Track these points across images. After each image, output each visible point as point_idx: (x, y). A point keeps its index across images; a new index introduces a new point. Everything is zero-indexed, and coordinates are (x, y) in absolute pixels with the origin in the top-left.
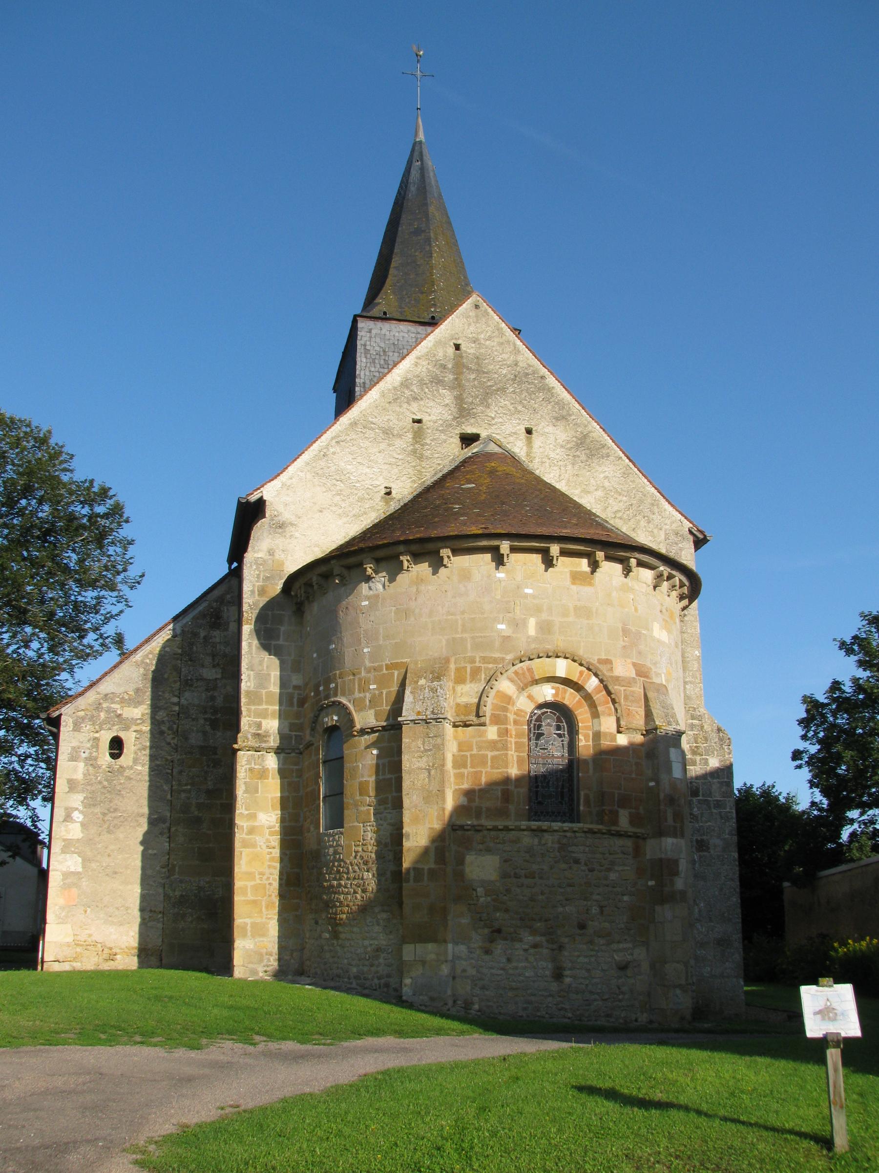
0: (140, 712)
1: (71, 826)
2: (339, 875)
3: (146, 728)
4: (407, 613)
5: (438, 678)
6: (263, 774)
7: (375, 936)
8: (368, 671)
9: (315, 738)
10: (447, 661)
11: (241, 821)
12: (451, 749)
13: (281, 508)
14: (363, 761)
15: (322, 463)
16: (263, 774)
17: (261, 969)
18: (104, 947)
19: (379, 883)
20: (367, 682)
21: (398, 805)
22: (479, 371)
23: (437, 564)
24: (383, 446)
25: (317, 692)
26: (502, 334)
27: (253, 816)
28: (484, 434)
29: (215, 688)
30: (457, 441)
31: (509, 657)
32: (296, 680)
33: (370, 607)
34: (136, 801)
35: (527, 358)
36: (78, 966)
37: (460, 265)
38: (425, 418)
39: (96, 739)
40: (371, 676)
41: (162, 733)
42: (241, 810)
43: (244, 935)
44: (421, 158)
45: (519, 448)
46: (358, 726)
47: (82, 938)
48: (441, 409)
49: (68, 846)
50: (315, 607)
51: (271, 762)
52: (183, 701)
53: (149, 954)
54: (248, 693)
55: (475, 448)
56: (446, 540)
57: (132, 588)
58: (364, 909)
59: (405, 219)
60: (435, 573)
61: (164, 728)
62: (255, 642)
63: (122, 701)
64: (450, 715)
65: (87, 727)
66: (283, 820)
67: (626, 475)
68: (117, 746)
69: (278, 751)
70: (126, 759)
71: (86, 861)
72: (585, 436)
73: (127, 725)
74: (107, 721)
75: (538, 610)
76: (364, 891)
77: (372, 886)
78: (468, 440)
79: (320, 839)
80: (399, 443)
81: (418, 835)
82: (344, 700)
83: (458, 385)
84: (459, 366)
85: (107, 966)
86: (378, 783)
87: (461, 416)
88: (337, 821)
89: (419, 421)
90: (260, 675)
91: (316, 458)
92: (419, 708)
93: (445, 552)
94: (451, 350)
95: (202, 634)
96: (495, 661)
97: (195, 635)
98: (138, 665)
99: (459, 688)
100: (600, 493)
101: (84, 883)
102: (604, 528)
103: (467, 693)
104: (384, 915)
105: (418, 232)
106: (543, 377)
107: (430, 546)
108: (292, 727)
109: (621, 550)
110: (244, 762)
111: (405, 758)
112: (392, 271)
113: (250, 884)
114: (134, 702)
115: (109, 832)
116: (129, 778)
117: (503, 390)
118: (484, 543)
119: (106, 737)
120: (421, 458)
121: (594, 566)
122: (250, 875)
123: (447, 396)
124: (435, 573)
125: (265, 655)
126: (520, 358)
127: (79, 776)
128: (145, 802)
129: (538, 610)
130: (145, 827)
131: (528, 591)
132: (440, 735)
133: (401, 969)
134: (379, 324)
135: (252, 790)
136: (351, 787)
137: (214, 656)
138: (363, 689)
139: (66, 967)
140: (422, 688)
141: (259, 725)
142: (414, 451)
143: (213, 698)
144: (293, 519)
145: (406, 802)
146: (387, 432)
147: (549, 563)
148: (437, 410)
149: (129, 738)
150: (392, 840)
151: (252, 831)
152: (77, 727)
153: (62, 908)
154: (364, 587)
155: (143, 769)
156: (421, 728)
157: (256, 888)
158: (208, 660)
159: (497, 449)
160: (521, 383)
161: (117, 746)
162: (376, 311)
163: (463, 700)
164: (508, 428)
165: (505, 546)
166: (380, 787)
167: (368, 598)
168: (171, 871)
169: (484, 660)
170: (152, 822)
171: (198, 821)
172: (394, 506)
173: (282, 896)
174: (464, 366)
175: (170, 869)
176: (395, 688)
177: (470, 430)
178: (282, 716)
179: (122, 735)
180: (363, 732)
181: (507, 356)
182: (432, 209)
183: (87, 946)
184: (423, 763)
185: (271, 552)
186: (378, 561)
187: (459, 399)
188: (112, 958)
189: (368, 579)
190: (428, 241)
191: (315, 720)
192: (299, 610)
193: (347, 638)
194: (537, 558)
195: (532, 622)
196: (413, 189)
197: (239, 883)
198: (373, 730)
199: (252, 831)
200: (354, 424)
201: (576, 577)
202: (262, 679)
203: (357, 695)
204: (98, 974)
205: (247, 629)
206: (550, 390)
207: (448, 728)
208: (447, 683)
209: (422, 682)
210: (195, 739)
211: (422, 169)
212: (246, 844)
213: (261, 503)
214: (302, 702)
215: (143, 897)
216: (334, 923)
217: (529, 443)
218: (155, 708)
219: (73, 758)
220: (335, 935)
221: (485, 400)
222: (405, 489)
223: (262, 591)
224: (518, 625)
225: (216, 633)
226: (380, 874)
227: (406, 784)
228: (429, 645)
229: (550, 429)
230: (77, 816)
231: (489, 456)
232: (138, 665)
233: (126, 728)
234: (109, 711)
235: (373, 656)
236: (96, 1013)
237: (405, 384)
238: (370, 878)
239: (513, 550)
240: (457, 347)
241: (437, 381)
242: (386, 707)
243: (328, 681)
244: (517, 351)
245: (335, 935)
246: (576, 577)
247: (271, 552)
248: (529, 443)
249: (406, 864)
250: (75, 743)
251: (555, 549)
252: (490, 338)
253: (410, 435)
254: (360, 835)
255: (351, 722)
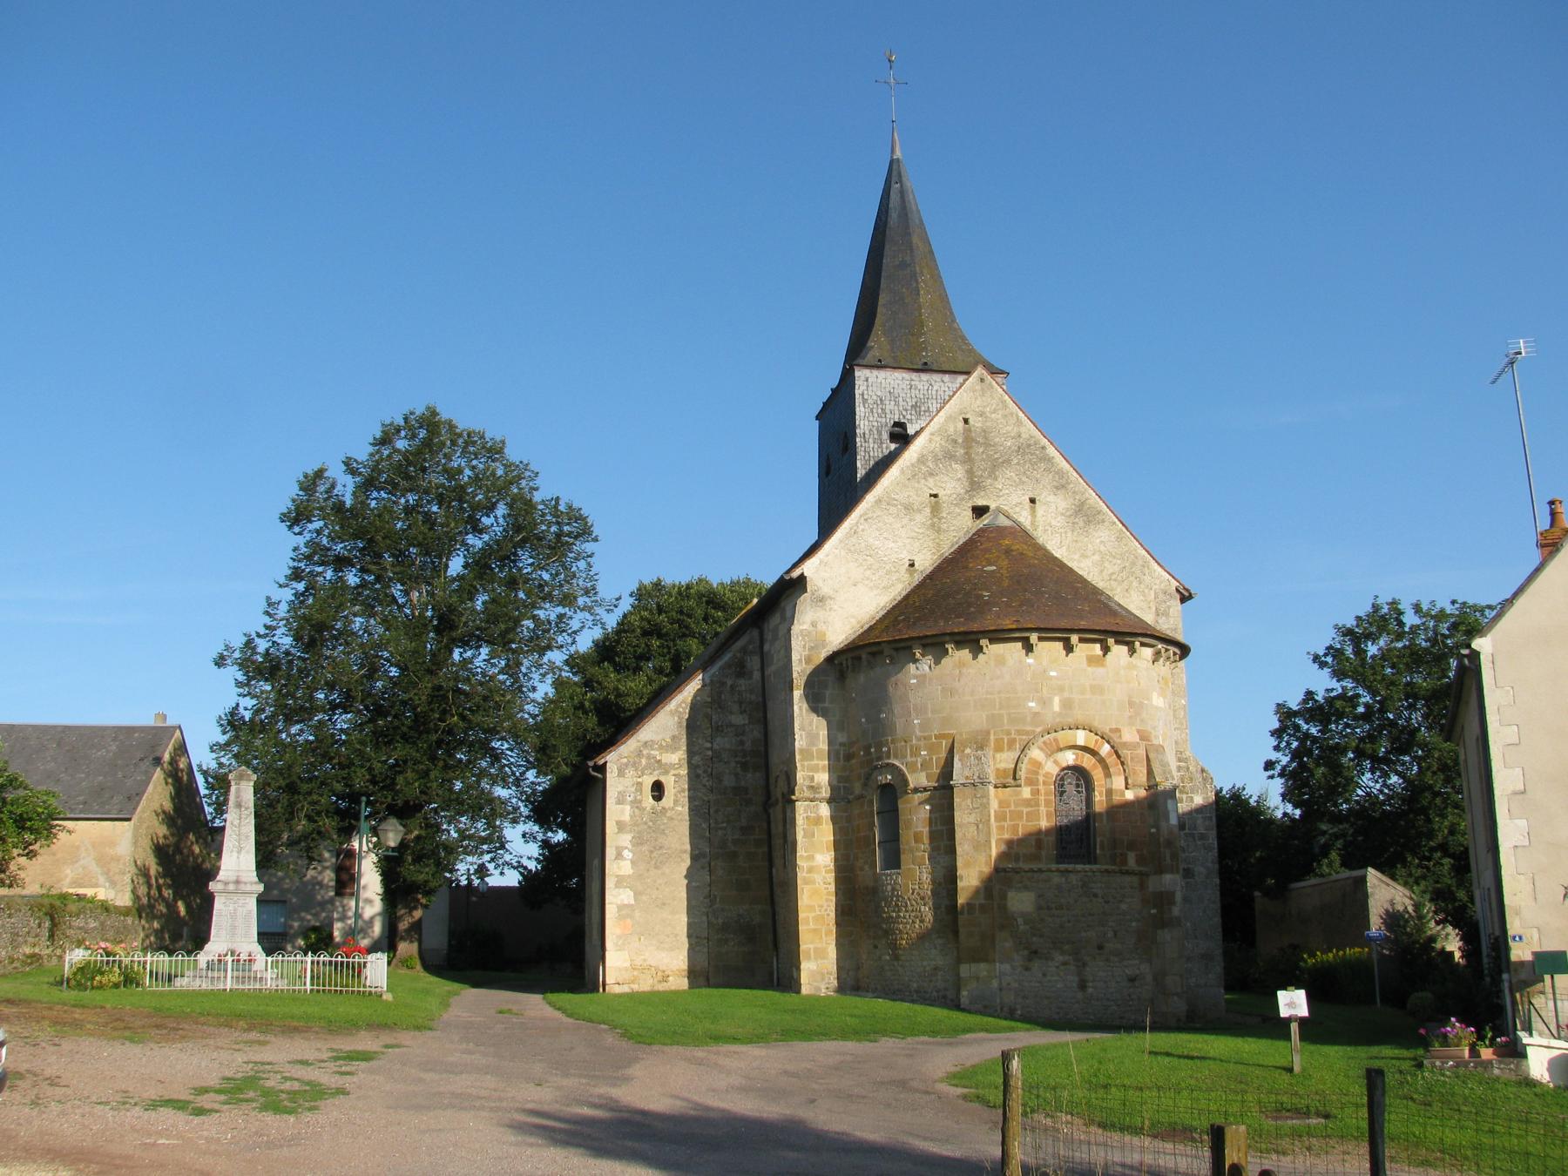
0: (677, 757)
1: (622, 863)
2: (898, 908)
3: (684, 772)
4: (952, 692)
5: (982, 748)
6: (818, 821)
7: (936, 957)
8: (919, 739)
9: (870, 797)
10: (988, 733)
11: (802, 862)
12: (994, 805)
13: (820, 584)
14: (917, 816)
15: (854, 540)
16: (818, 821)
17: (823, 987)
18: (657, 969)
19: (935, 916)
20: (918, 749)
21: (952, 851)
22: (987, 445)
23: (977, 650)
24: (905, 521)
25: (868, 753)
26: (1006, 407)
27: (811, 858)
28: (993, 506)
29: (743, 734)
30: (970, 513)
31: (1039, 730)
32: (842, 738)
33: (918, 685)
34: (678, 838)
35: (1029, 429)
36: (636, 987)
37: (944, 299)
38: (941, 493)
39: (640, 784)
40: (922, 743)
41: (698, 776)
42: (801, 852)
43: (809, 958)
44: (900, 181)
45: (1024, 518)
46: (912, 786)
47: (638, 962)
48: (954, 484)
49: (621, 881)
50: (862, 678)
51: (825, 810)
52: (716, 747)
53: (698, 975)
54: (801, 751)
55: (986, 520)
56: (985, 633)
57: (608, 611)
58: (923, 937)
59: (889, 250)
60: (975, 658)
61: (700, 772)
62: (805, 706)
63: (661, 748)
64: (992, 779)
65: (630, 772)
66: (836, 860)
67: (1119, 539)
68: (658, 789)
69: (830, 801)
70: (667, 801)
71: (637, 894)
72: (1083, 504)
73: (666, 769)
74: (648, 766)
75: (1061, 689)
76: (922, 921)
77: (929, 916)
78: (979, 511)
79: (876, 878)
80: (919, 518)
81: (970, 876)
82: (897, 763)
83: (968, 459)
84: (969, 440)
85: (661, 987)
86: (931, 832)
87: (972, 489)
88: (893, 860)
89: (935, 496)
90: (810, 735)
91: (848, 536)
92: (967, 773)
93: (984, 642)
94: (961, 424)
95: (729, 683)
96: (1027, 733)
97: (724, 684)
98: (672, 713)
99: (998, 756)
100: (1097, 557)
101: (637, 914)
102: (1114, 614)
103: (1005, 760)
104: (940, 941)
105: (903, 265)
106: (1043, 448)
107: (973, 637)
108: (840, 779)
109: (1130, 633)
110: (802, 811)
111: (957, 814)
112: (879, 309)
113: (812, 915)
114: (672, 748)
115: (656, 868)
116: (671, 819)
117: (1008, 461)
118: (1017, 635)
119: (648, 781)
120: (939, 531)
121: (1106, 650)
122: (811, 908)
123: (959, 470)
124: (975, 658)
125: (814, 717)
126: (1023, 430)
127: (626, 817)
128: (687, 840)
129: (1061, 689)
130: (688, 862)
131: (1053, 674)
132: (986, 796)
133: (958, 984)
134: (875, 372)
135: (809, 835)
136: (906, 837)
137: (741, 703)
138: (916, 753)
139: (625, 989)
140: (968, 756)
141: (812, 779)
142: (933, 525)
143: (742, 743)
144: (831, 593)
145: (959, 849)
146: (908, 508)
147: (1069, 649)
148: (951, 484)
149: (669, 782)
150: (947, 880)
151: (810, 870)
152: (621, 773)
153: (619, 937)
154: (912, 666)
155: (683, 809)
156: (969, 790)
157: (816, 919)
158: (736, 708)
159: (1007, 523)
160: (1024, 454)
161: (658, 789)
162: (870, 357)
163: (1002, 766)
164: (1014, 499)
165: (1034, 637)
166: (933, 836)
167: (915, 677)
168: (713, 902)
169: (1019, 732)
170: (694, 858)
171: (734, 855)
172: (917, 578)
173: (838, 924)
174: (973, 440)
175: (711, 898)
176: (943, 755)
177: (981, 502)
178: (831, 769)
179: (662, 779)
180: (916, 790)
181: (1011, 429)
182: (915, 239)
183: (643, 970)
184: (972, 819)
185: (814, 624)
186: (924, 646)
187: (970, 473)
188: (665, 979)
189: (916, 661)
190: (914, 276)
191: (868, 777)
192: (842, 676)
193: (897, 710)
194: (1059, 645)
195: (1056, 700)
196: (894, 216)
197: (802, 915)
198: (925, 790)
199: (810, 870)
200: (879, 501)
201: (1091, 660)
202: (813, 738)
203: (909, 759)
204: (653, 993)
205: (798, 694)
206: (1050, 460)
207: (991, 788)
208: (989, 752)
209: (968, 751)
210: (729, 781)
211: (902, 192)
212: (806, 882)
213: (802, 578)
214: (848, 757)
215: (690, 925)
216: (894, 946)
217: (1033, 511)
218: (691, 753)
219: (620, 802)
220: (896, 957)
221: (992, 474)
222: (926, 561)
223: (808, 660)
224: (1045, 702)
225: (741, 681)
226: (936, 908)
227: (958, 835)
228: (971, 719)
229: (1051, 498)
230: (627, 854)
231: (1001, 531)
232: (672, 713)
233: (666, 773)
234: (649, 757)
235: (923, 727)
236: (650, 1024)
237: (922, 460)
238: (927, 912)
239: (1040, 639)
240: (966, 421)
241: (950, 456)
242: (936, 771)
243: (879, 745)
244: (1019, 423)
245: (896, 957)
246: (1091, 660)
247: (814, 624)
248: (1033, 511)
249: (961, 901)
250: (621, 788)
251: (1074, 638)
252: (994, 411)
253: (928, 510)
254: (917, 875)
255: (906, 782)
